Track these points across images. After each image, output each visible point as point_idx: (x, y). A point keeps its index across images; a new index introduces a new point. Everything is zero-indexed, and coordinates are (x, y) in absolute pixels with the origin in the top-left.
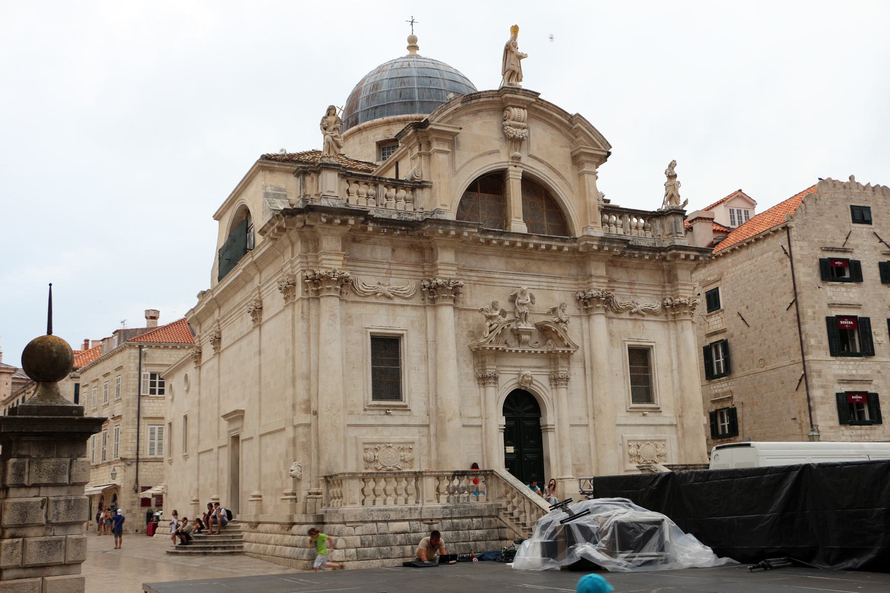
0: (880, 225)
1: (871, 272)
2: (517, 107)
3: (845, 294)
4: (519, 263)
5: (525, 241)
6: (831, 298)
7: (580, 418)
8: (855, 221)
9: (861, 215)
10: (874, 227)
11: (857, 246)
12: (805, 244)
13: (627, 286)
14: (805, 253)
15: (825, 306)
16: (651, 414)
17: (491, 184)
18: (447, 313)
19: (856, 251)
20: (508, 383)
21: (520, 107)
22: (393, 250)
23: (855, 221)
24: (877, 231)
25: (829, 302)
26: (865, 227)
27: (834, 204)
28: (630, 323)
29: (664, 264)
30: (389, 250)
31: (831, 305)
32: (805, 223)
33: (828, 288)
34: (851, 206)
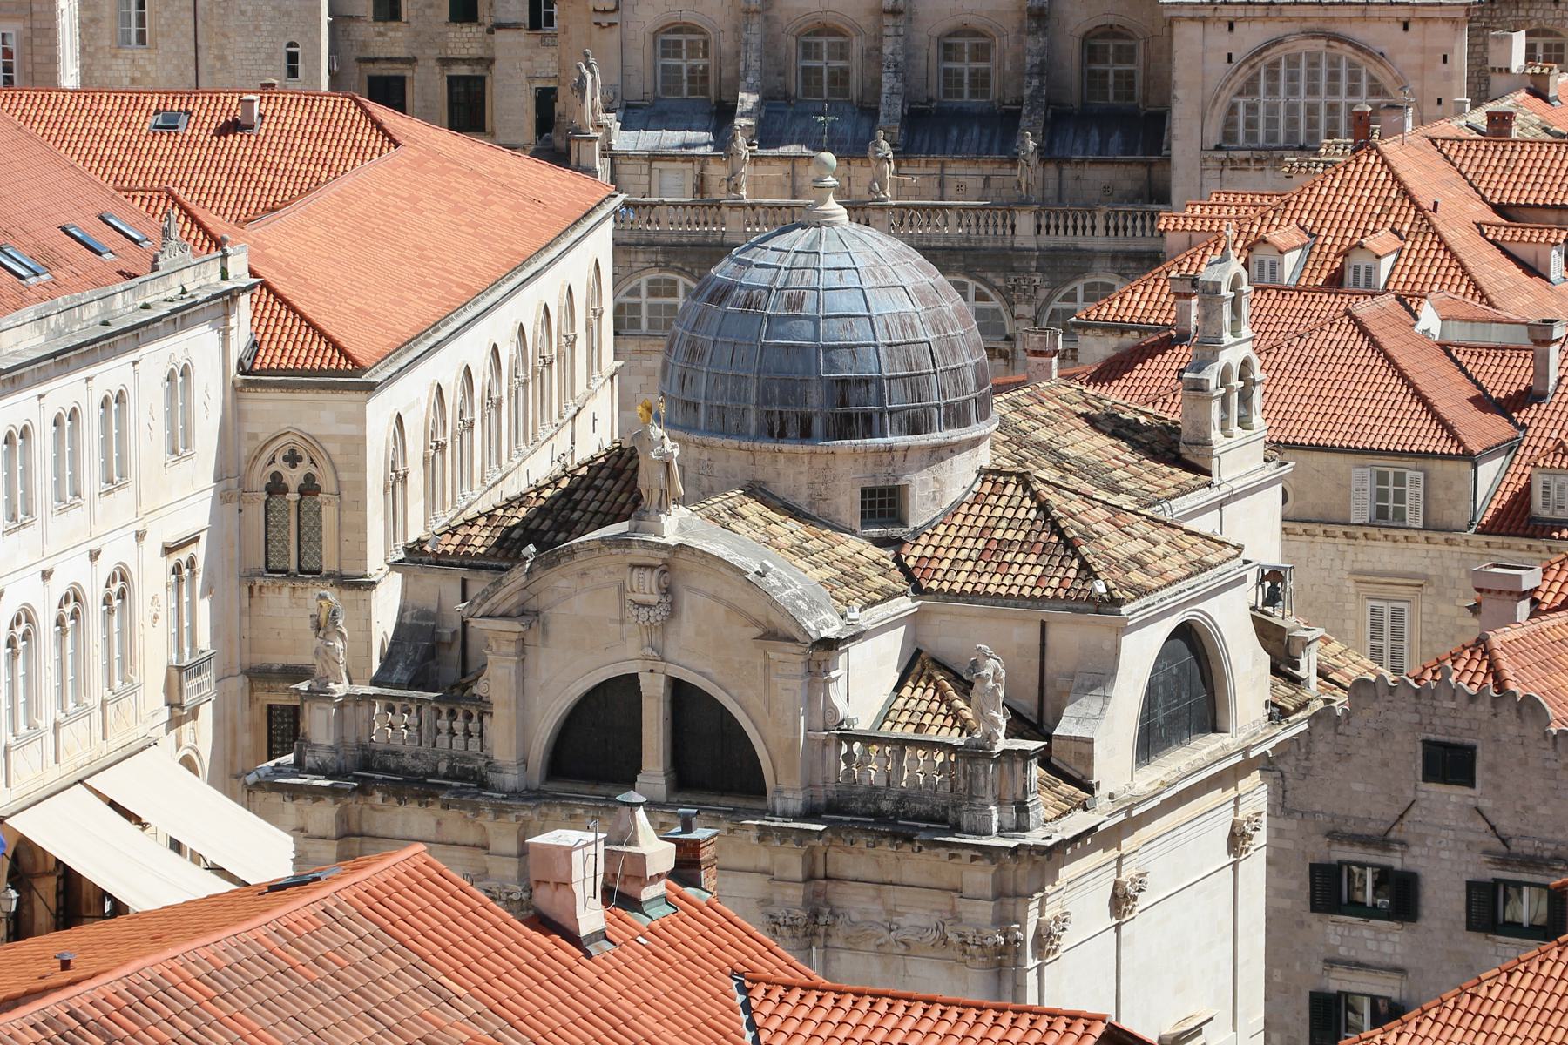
0: (1498, 787)
1: (1443, 898)
2: (640, 566)
3: (1371, 945)
6: (1335, 948)
8: (1430, 774)
9: (1449, 763)
10: (1476, 795)
11: (1422, 837)
12: (1290, 824)
14: (1289, 845)
15: (1318, 967)
17: (611, 702)
19: (1415, 850)
21: (647, 566)
22: (439, 823)
23: (1430, 774)
24: (1486, 804)
25: (1328, 955)
26: (1455, 793)
27: (1383, 734)
30: (433, 824)
31: (1331, 963)
32: (1306, 773)
33: (1331, 928)
34: (1426, 742)
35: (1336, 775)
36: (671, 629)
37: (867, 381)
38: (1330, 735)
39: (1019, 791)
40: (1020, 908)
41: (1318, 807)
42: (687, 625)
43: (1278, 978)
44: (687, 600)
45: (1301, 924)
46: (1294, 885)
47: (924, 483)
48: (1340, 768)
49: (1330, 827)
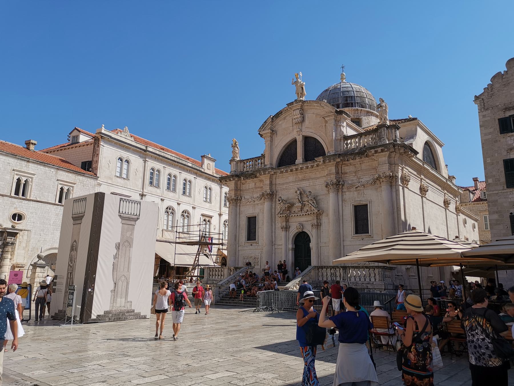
4: (301, 176)
5: (296, 167)
7: (325, 243)
13: (354, 174)
16: (366, 239)
18: (266, 205)
20: (294, 230)
28: (355, 193)
29: (373, 157)
30: (254, 184)
33: (509, 138)
35: (504, 91)
36: (303, 124)
37: (352, 97)
38: (500, 81)
39: (394, 137)
40: (396, 168)
41: (498, 104)
42: (307, 122)
43: (489, 160)
44: (307, 116)
45: (496, 141)
46: (492, 130)
47: (365, 119)
48: (505, 89)
49: (504, 107)
